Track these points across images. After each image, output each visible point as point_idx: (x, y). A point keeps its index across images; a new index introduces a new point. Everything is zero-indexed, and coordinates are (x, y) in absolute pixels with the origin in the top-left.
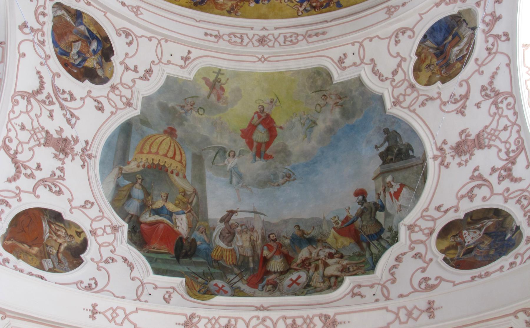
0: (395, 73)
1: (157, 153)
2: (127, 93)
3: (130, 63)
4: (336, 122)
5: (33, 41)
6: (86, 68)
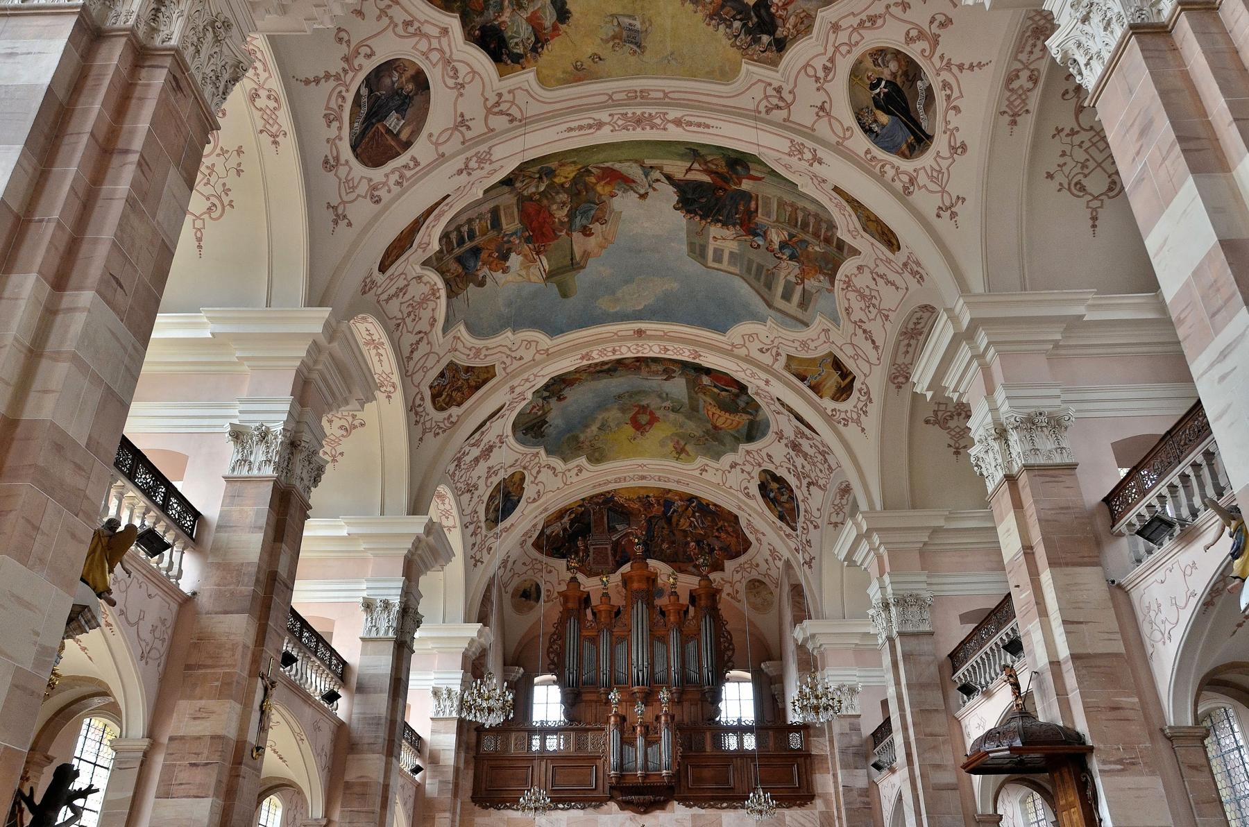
0: (539, 472)
1: (727, 419)
3: (745, 475)
4: (583, 432)
6: (778, 483)
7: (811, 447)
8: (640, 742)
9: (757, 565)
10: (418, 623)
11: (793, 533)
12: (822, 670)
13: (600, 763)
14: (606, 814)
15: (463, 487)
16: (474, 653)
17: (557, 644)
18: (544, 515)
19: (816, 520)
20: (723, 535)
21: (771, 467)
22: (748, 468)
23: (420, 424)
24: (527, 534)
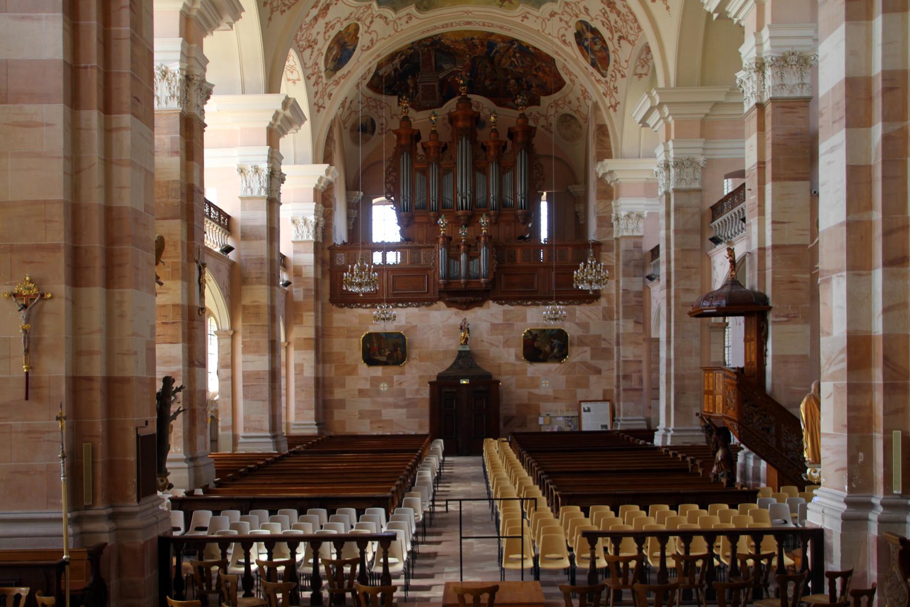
0: (371, 22)
2: (567, 9)
5: (620, 65)
7: (624, 6)
8: (463, 257)
9: (570, 102)
10: (282, 180)
11: (603, 79)
12: (617, 198)
13: (431, 273)
14: (436, 310)
15: (305, 44)
16: (322, 187)
17: (392, 175)
18: (379, 59)
19: (623, 70)
20: (541, 74)
21: (586, 19)
22: (566, 17)
23: (268, 6)
24: (363, 78)
